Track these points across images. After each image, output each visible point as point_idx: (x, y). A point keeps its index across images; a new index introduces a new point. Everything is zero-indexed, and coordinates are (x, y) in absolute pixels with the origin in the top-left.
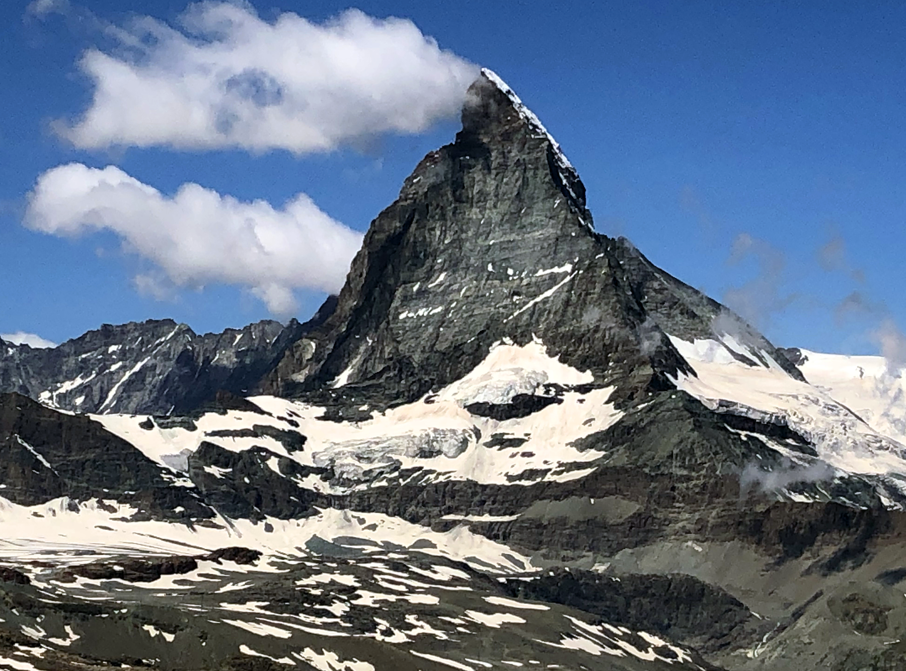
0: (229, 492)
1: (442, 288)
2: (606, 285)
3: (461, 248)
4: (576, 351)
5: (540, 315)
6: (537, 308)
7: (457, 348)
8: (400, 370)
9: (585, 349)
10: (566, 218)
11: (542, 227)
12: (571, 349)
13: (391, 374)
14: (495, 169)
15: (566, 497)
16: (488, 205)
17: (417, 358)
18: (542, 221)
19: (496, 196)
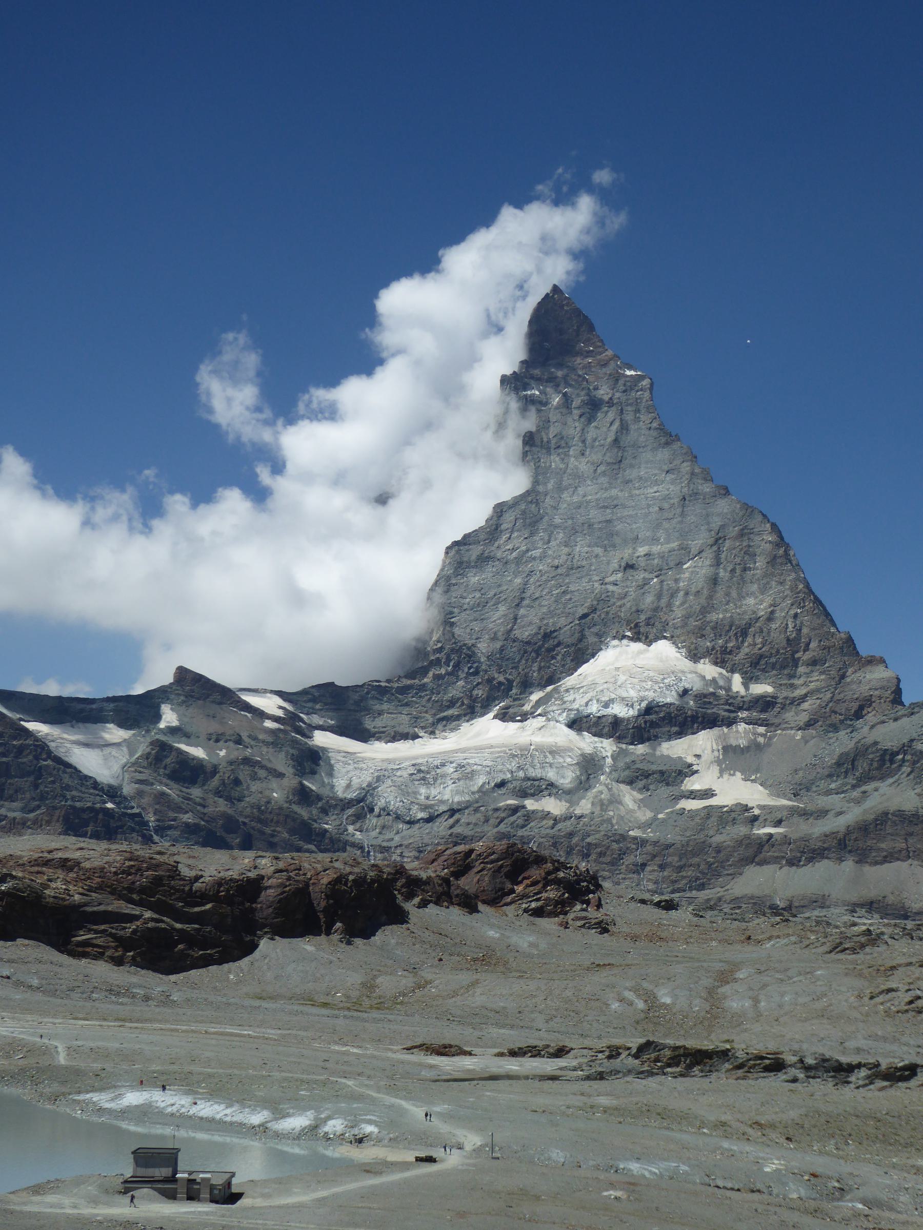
0: (196, 825)
1: (514, 554)
2: (775, 557)
3: (537, 503)
4: (739, 648)
5: (672, 596)
6: (665, 587)
7: (547, 636)
8: (457, 666)
9: (755, 644)
10: (693, 474)
11: (656, 483)
12: (730, 645)
13: (443, 671)
14: (579, 408)
15: (810, 860)
16: (571, 453)
17: (483, 647)
18: (656, 475)
19: (584, 441)
